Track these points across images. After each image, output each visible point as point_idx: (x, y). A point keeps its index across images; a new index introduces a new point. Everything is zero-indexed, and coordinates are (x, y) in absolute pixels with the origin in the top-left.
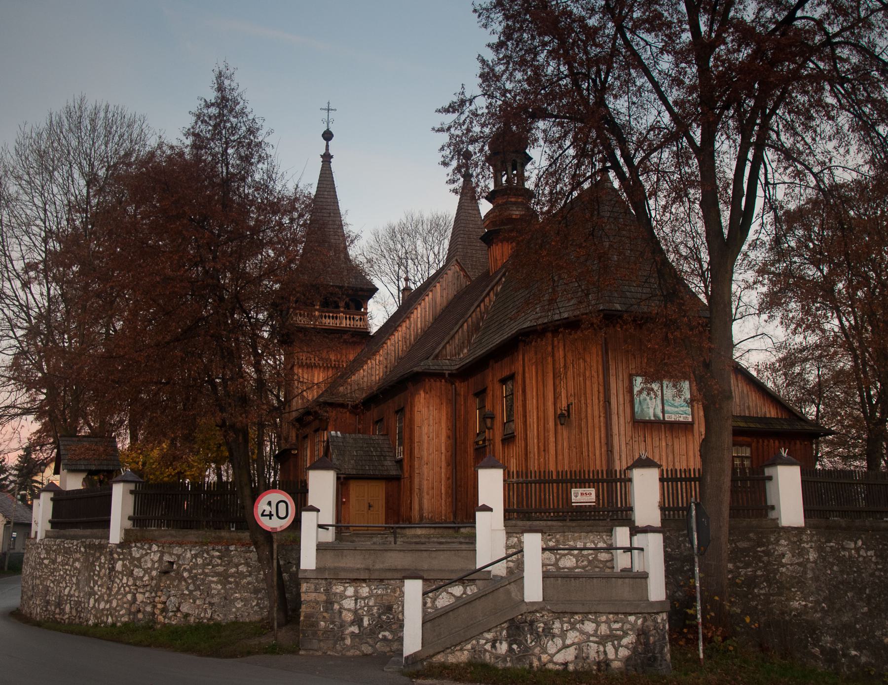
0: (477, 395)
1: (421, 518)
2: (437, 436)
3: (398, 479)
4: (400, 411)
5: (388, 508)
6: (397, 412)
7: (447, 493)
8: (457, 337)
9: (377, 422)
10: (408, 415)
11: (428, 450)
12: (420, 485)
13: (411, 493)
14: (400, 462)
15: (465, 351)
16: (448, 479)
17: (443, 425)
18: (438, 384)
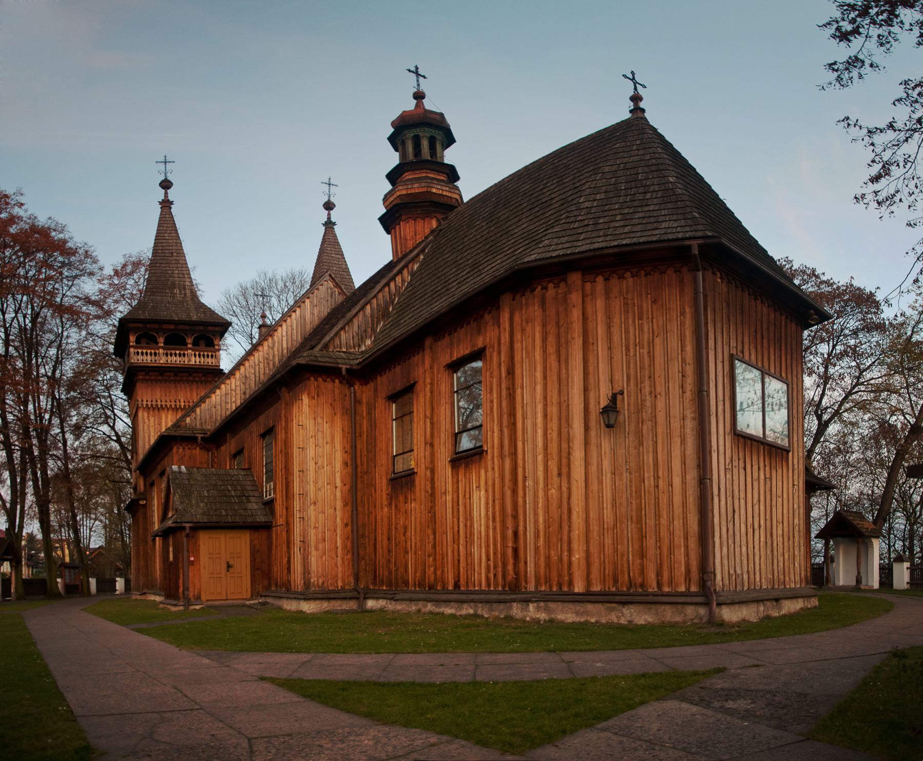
0: (393, 398)
1: (307, 584)
2: (330, 463)
3: (267, 527)
4: (269, 432)
5: (255, 567)
6: (263, 436)
7: (344, 546)
8: (355, 321)
9: (235, 456)
10: (281, 436)
11: (316, 482)
12: (304, 535)
13: (288, 547)
14: (270, 504)
15: (368, 342)
16: (346, 525)
17: (338, 446)
18: (329, 385)
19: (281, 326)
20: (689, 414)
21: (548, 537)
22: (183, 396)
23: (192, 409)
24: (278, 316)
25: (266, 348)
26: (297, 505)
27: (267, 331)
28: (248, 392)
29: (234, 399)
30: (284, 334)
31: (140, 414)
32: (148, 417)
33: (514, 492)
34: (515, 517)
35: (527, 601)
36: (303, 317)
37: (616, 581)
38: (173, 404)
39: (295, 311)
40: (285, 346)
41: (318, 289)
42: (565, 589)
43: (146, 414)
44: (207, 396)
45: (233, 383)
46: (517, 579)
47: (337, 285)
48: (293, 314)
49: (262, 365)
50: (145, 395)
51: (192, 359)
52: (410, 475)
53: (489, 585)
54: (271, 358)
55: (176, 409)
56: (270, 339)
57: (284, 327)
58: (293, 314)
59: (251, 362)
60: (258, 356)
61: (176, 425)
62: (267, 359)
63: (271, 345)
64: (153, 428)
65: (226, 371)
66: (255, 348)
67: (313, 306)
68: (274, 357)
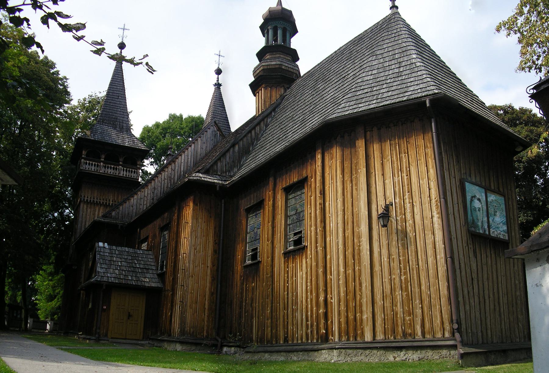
19: (181, 155)
22: (111, 198)
23: (117, 207)
25: (170, 170)
28: (155, 198)
29: (145, 203)
30: (183, 161)
31: (82, 205)
32: (87, 209)
38: (105, 202)
39: (191, 146)
40: (182, 169)
41: (207, 132)
43: (85, 206)
44: (128, 199)
45: (147, 192)
46: (327, 333)
48: (190, 148)
49: (166, 181)
50: (87, 194)
54: (173, 177)
56: (173, 165)
57: (183, 156)
58: (190, 148)
59: (159, 179)
62: (170, 177)
63: (173, 168)
68: (174, 176)
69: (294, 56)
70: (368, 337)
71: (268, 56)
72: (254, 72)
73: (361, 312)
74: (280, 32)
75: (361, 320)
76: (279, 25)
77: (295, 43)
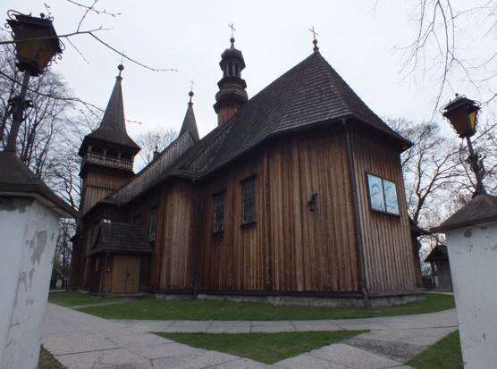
17: (188, 217)
20: (348, 203)
21: (285, 263)
22: (111, 183)
24: (163, 149)
26: (166, 244)
27: (158, 156)
31: (88, 189)
33: (270, 242)
34: (270, 254)
35: (275, 295)
36: (175, 149)
37: (317, 286)
42: (294, 290)
44: (125, 185)
45: (139, 180)
47: (192, 137)
50: (92, 180)
51: (120, 164)
52: (221, 233)
53: (257, 286)
55: (107, 189)
60: (152, 168)
61: (107, 198)
64: (96, 197)
65: (136, 173)
66: (150, 165)
67: (180, 146)
69: (243, 84)
70: (300, 289)
71: (226, 85)
72: (216, 96)
73: (295, 270)
74: (234, 68)
75: (295, 277)
76: (232, 61)
77: (244, 75)
